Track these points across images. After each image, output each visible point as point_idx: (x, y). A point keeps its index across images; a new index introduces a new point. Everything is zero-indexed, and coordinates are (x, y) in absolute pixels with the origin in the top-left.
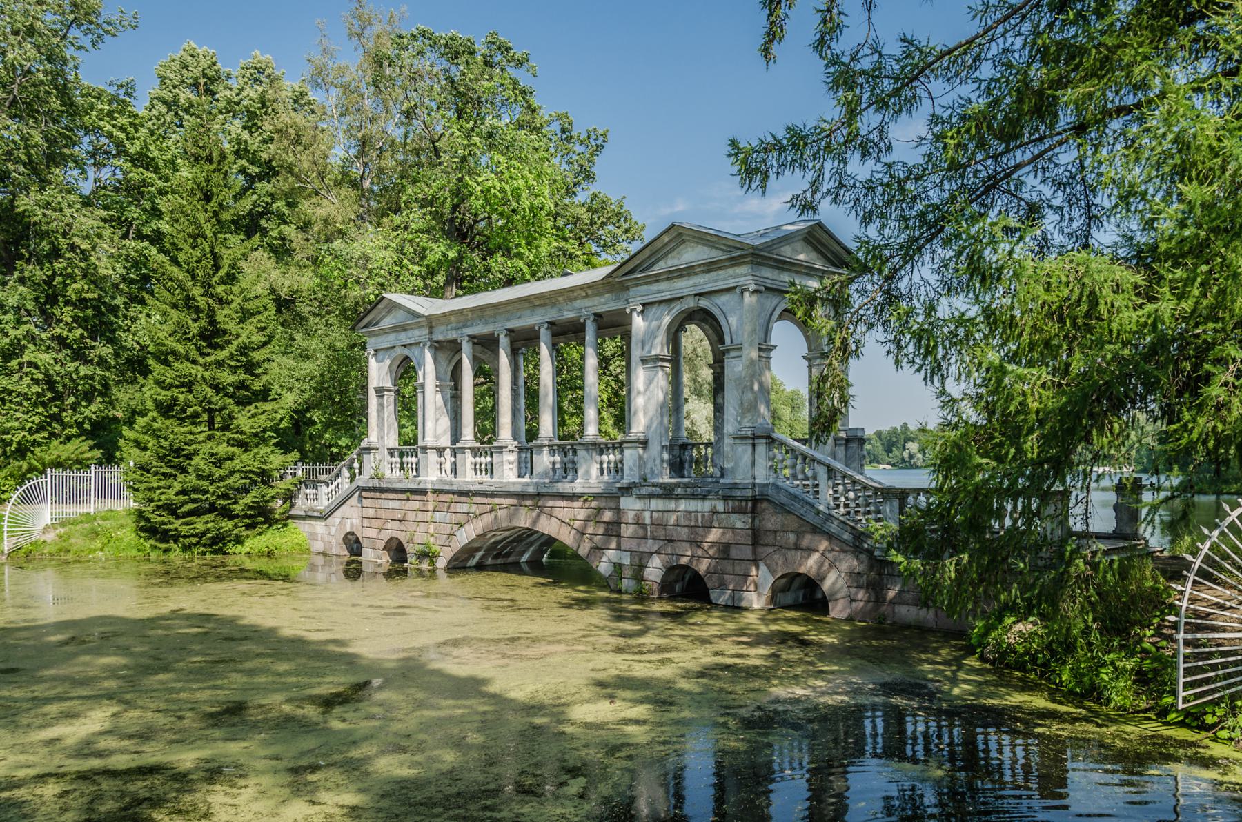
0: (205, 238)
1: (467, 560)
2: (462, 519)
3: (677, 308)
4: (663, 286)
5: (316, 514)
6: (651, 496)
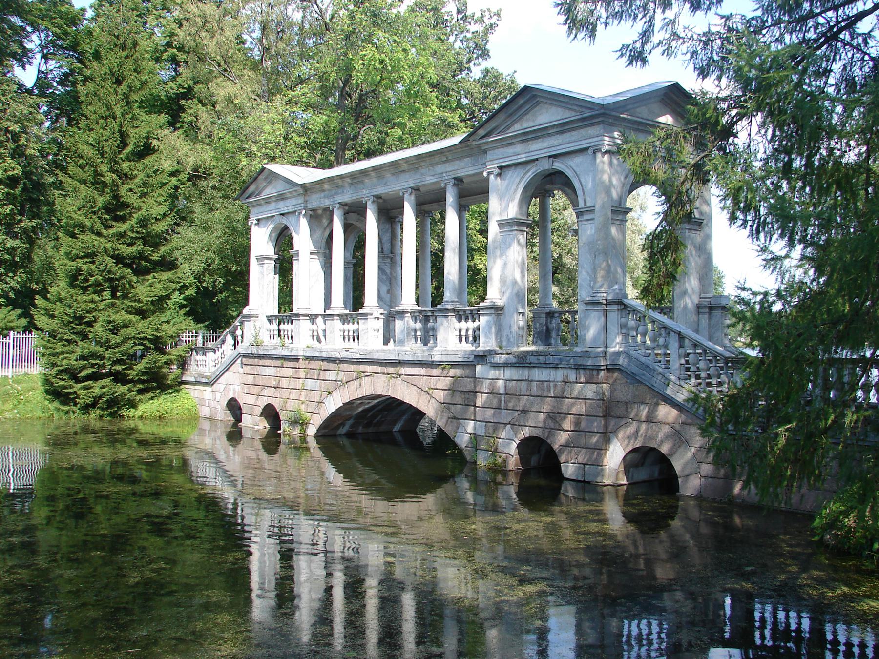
0: (115, 118)
1: (338, 427)
2: (329, 386)
4: (519, 148)
5: (204, 380)
6: (506, 365)
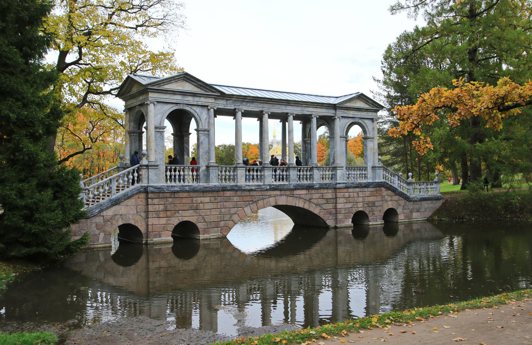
3: (351, 121)
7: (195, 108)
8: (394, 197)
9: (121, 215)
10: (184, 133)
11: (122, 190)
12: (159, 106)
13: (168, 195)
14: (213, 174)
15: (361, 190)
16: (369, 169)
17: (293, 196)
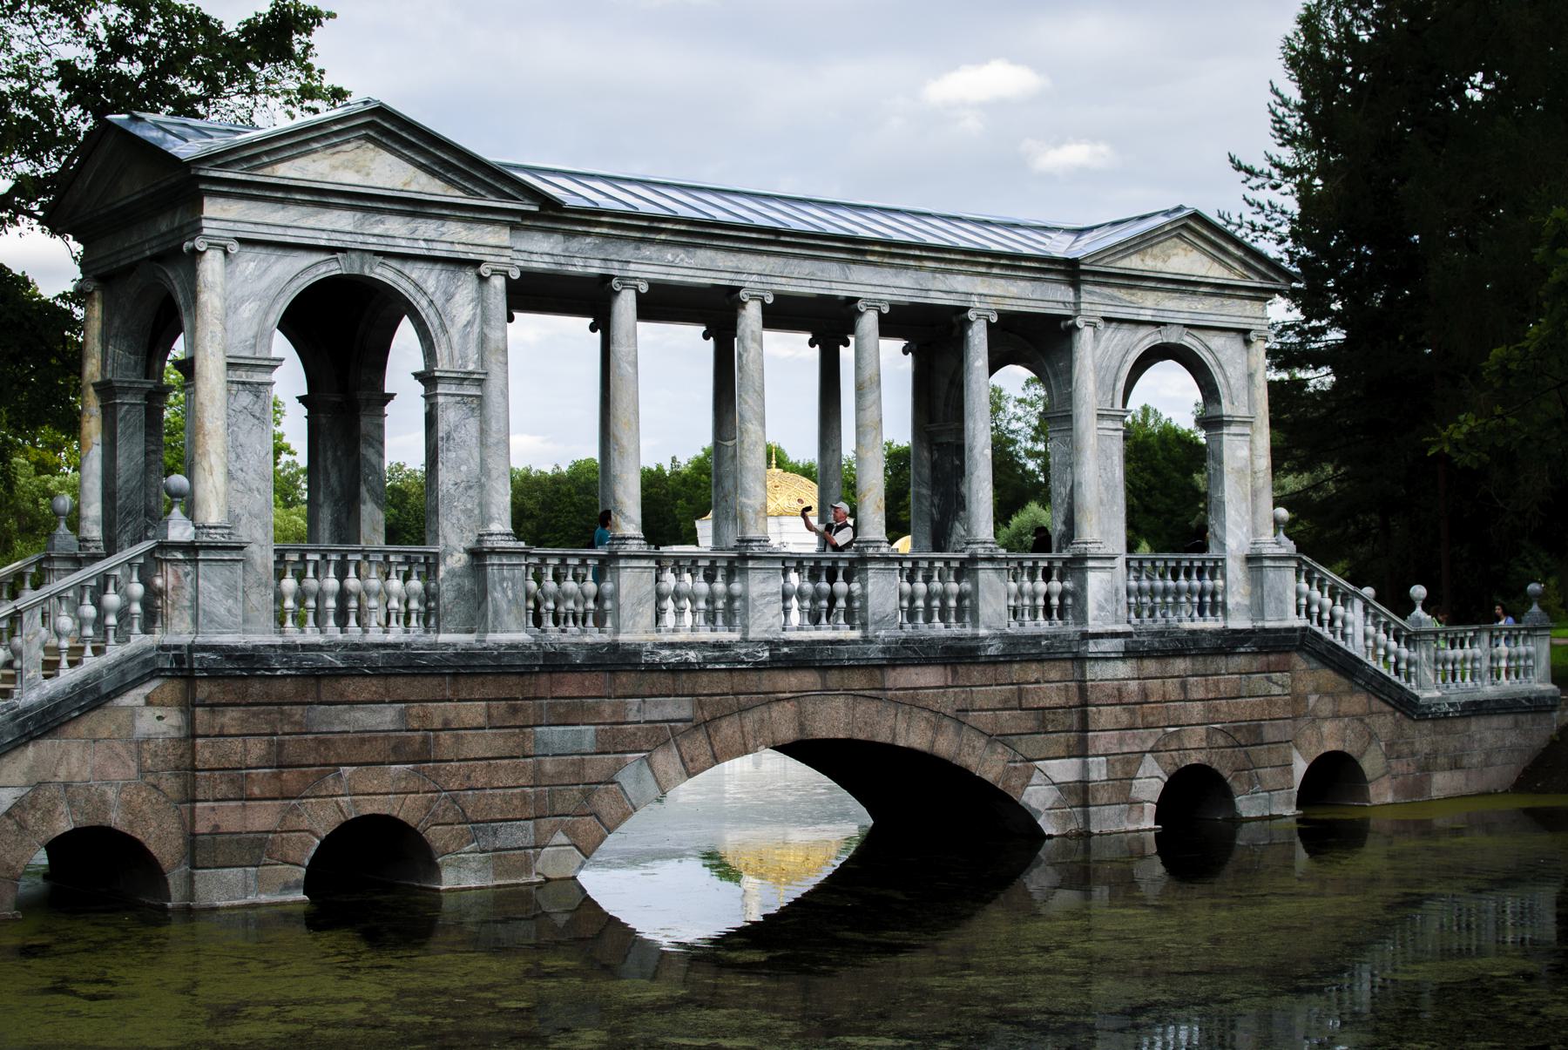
3: (1147, 339)
7: (416, 271)
8: (1346, 698)
9: (67, 785)
10: (362, 395)
11: (72, 664)
12: (250, 263)
13: (289, 688)
14: (504, 591)
15: (1199, 665)
16: (1235, 570)
17: (878, 694)
